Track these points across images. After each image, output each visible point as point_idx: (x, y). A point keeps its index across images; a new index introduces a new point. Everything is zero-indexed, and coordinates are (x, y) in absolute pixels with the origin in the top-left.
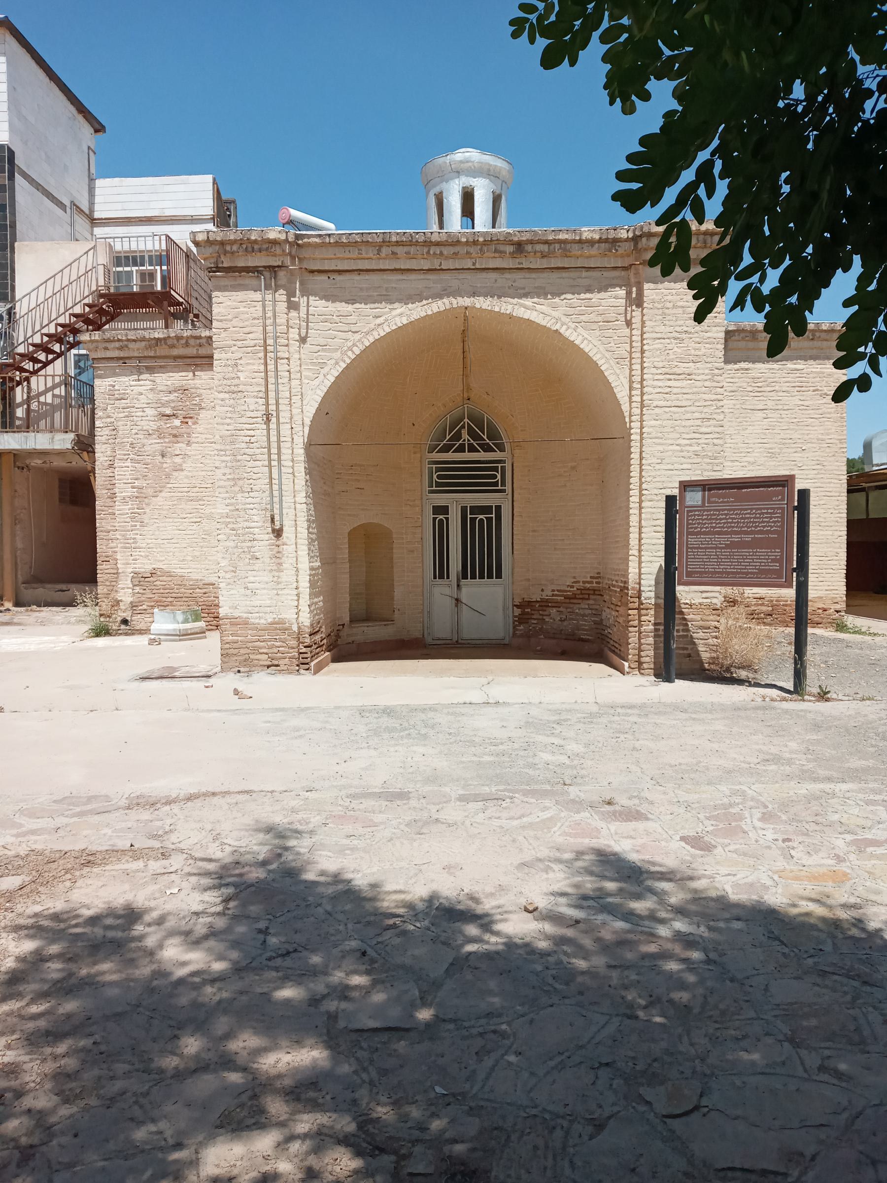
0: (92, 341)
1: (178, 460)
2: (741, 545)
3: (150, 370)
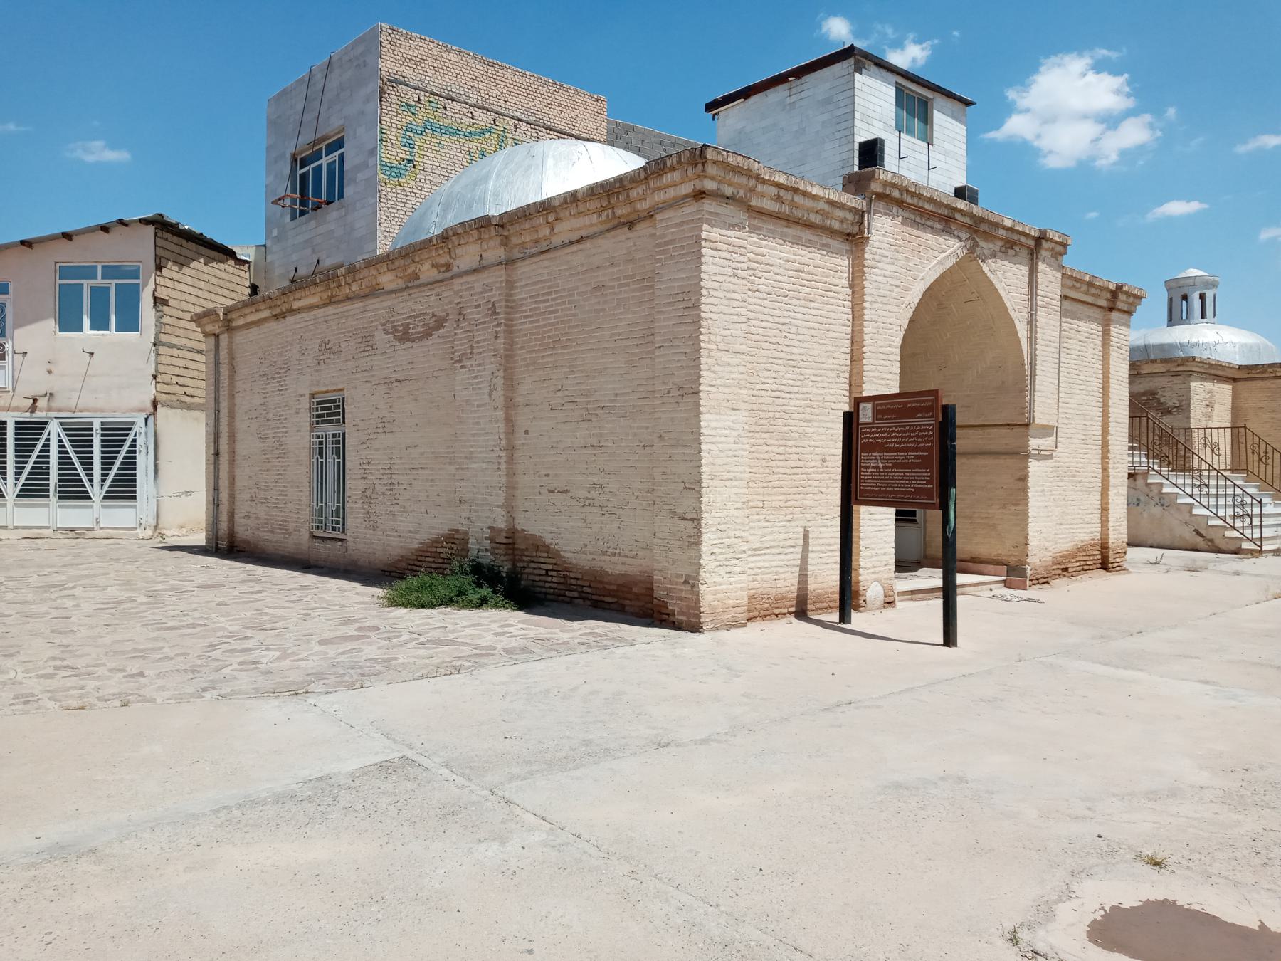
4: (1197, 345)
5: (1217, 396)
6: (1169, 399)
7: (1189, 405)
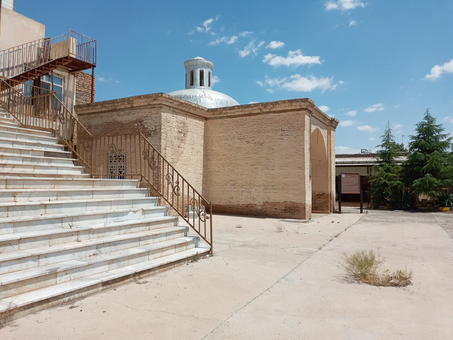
0: (165, 97)
1: (182, 149)
2: (352, 185)
3: (177, 113)
4: (189, 97)
5: (190, 127)
6: (149, 125)
7: (160, 129)
